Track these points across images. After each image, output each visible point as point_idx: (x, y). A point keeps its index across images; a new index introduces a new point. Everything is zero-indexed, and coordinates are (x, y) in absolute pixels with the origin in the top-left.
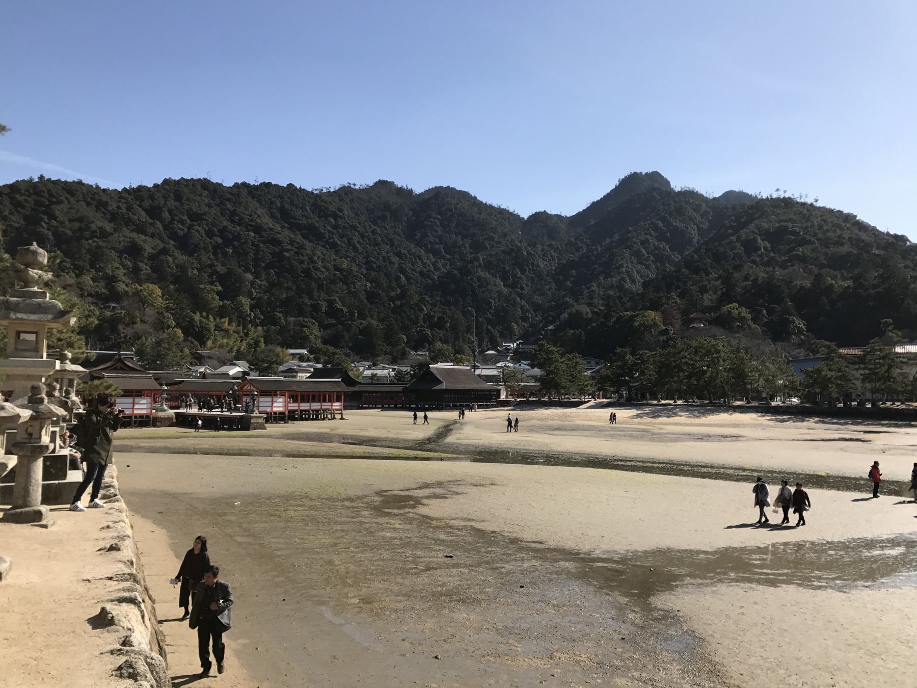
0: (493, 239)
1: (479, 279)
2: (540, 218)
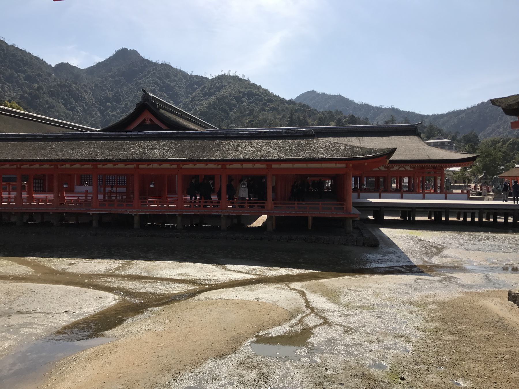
0: (42, 77)
1: (47, 102)
2: (64, 67)
